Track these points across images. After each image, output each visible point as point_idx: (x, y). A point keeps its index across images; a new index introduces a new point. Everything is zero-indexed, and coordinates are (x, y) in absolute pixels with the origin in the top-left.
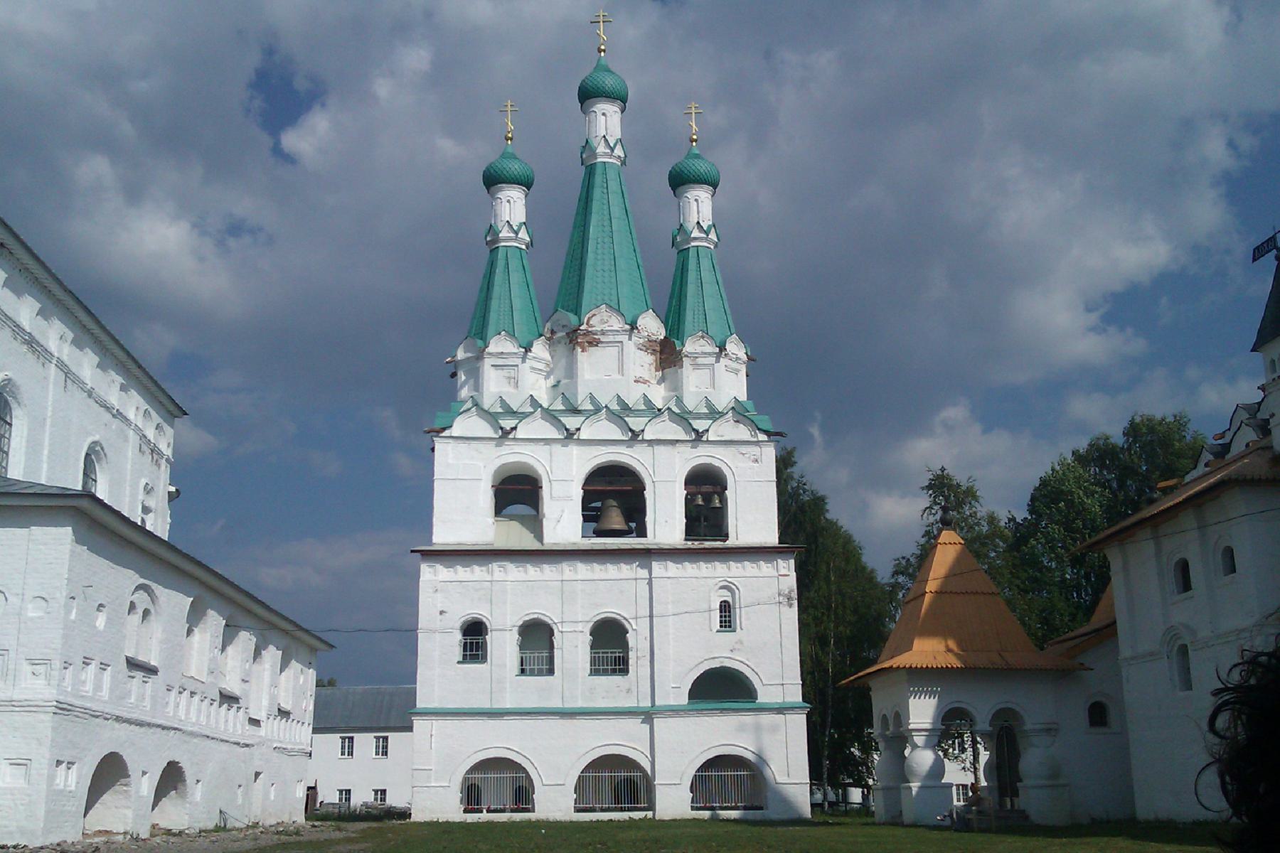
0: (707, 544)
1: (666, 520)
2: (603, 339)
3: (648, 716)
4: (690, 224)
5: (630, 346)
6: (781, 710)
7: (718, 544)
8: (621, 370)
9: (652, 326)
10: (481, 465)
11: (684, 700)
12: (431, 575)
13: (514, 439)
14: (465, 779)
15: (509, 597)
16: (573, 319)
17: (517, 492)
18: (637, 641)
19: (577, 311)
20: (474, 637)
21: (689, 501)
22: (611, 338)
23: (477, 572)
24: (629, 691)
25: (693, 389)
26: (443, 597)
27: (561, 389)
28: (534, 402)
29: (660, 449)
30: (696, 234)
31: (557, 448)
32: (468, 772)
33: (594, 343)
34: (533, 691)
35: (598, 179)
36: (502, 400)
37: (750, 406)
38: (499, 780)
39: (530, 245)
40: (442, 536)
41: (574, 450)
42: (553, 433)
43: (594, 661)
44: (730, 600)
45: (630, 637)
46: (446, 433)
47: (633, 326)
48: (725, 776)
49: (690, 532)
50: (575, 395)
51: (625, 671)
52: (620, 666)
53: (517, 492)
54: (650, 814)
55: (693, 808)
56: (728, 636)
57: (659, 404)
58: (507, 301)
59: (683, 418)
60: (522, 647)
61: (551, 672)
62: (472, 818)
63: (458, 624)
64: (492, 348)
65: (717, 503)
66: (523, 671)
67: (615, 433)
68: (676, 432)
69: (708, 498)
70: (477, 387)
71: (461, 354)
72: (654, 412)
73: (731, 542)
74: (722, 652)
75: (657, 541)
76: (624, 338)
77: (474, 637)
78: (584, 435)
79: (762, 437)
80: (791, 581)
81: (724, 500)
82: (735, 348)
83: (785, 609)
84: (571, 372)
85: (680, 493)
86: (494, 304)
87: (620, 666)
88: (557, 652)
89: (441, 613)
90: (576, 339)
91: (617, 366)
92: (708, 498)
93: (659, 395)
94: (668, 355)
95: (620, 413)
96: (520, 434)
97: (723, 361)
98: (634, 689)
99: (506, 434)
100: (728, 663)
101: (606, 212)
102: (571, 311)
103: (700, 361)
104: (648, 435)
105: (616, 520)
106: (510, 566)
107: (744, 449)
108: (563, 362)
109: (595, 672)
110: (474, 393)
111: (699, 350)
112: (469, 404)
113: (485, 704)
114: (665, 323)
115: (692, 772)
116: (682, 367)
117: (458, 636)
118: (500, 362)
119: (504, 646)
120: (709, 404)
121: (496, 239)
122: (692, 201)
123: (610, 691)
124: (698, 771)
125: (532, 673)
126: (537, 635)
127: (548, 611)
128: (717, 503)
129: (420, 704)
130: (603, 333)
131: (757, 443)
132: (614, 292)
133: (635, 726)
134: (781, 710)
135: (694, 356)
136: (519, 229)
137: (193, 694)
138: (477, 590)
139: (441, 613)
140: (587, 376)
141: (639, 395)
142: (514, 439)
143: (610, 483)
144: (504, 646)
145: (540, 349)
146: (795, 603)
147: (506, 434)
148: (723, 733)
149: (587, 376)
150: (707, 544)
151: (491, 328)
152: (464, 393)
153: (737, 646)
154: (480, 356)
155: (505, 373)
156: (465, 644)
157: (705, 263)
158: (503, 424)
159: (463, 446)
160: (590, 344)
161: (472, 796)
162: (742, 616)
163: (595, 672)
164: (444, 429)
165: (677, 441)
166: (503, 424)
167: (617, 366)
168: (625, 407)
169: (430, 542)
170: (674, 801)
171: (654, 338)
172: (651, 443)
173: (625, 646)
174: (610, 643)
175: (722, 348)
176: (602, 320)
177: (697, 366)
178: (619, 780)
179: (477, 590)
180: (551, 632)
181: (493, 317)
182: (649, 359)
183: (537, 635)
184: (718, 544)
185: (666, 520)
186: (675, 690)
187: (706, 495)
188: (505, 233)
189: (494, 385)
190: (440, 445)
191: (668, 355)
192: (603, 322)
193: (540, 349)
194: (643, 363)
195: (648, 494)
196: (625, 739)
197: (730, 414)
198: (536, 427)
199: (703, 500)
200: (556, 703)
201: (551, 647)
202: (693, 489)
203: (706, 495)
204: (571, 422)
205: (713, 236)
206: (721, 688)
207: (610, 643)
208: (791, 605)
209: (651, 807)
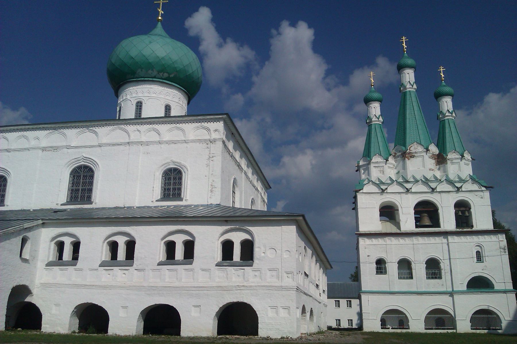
0: (465, 230)
1: (448, 220)
2: (416, 155)
3: (451, 294)
4: (445, 111)
5: (427, 157)
6: (505, 292)
7: (469, 230)
8: (424, 166)
9: (434, 149)
11: (465, 288)
12: (363, 242)
13: (387, 193)
14: (382, 317)
15: (394, 250)
16: (404, 148)
17: (388, 212)
18: (444, 266)
19: (404, 145)
21: (456, 214)
22: (419, 155)
23: (380, 241)
24: (442, 285)
25: (452, 172)
26: (369, 251)
27: (400, 174)
28: (391, 179)
29: (443, 195)
30: (447, 114)
31: (404, 196)
32: (383, 314)
33: (413, 157)
34: (405, 285)
35: (408, 97)
36: (379, 179)
38: (396, 317)
39: (383, 123)
40: (363, 228)
41: (410, 196)
42: (401, 190)
44: (480, 250)
45: (442, 265)
46: (361, 191)
47: (427, 150)
49: (458, 225)
50: (407, 176)
53: (388, 212)
54: (455, 331)
55: (472, 329)
57: (439, 178)
59: (450, 182)
61: (411, 278)
63: (375, 261)
64: (374, 160)
65: (467, 214)
67: (425, 189)
68: (449, 188)
70: (369, 174)
71: (361, 163)
72: (440, 181)
73: (474, 229)
75: (445, 229)
76: (424, 154)
77: (381, 266)
79: (484, 189)
80: (504, 243)
81: (470, 213)
82: (467, 156)
84: (404, 167)
85: (453, 211)
86: (372, 145)
88: (414, 271)
90: (405, 155)
93: (438, 174)
94: (441, 160)
95: (426, 182)
96: (389, 190)
97: (463, 161)
99: (383, 191)
100: (481, 274)
101: (412, 109)
102: (402, 145)
103: (454, 161)
104: (438, 189)
105: (427, 221)
106: (393, 239)
107: (477, 193)
108: (401, 163)
109: (428, 278)
110: (368, 177)
111: (453, 157)
112: (366, 182)
113: (388, 290)
115: (470, 315)
116: (447, 164)
117: (375, 265)
118: (377, 165)
119: (392, 268)
120: (459, 177)
121: (371, 121)
122: (445, 102)
123: (434, 285)
125: (404, 278)
126: (405, 265)
127: (410, 256)
128: (467, 214)
129: (363, 289)
130: (416, 153)
131: (482, 191)
133: (447, 299)
134: (505, 292)
135: (451, 160)
139: (368, 256)
142: (387, 193)
144: (392, 268)
145: (391, 160)
146: (507, 251)
147: (383, 191)
150: (465, 230)
151: (372, 154)
152: (363, 177)
154: (369, 163)
155: (379, 169)
157: (452, 125)
158: (381, 187)
159: (368, 196)
160: (411, 157)
161: (383, 323)
163: (428, 278)
164: (360, 190)
165: (450, 191)
166: (381, 187)
168: (426, 179)
169: (359, 231)
170: (464, 326)
172: (440, 192)
173: (439, 268)
174: (433, 267)
175: (463, 156)
176: (415, 148)
177: (452, 163)
181: (372, 150)
182: (433, 161)
183: (405, 265)
184: (469, 230)
185: (448, 220)
187: (463, 211)
188: (374, 119)
189: (375, 173)
190: (359, 196)
191: (441, 160)
192: (415, 149)
193: (391, 160)
194: (431, 163)
195: (440, 211)
196: (443, 303)
197: (470, 180)
199: (462, 213)
200: (414, 289)
202: (457, 209)
203: (463, 211)
204: (408, 186)
205: (454, 115)
206: (480, 284)
207: (433, 267)
208: (505, 252)
209: (455, 328)
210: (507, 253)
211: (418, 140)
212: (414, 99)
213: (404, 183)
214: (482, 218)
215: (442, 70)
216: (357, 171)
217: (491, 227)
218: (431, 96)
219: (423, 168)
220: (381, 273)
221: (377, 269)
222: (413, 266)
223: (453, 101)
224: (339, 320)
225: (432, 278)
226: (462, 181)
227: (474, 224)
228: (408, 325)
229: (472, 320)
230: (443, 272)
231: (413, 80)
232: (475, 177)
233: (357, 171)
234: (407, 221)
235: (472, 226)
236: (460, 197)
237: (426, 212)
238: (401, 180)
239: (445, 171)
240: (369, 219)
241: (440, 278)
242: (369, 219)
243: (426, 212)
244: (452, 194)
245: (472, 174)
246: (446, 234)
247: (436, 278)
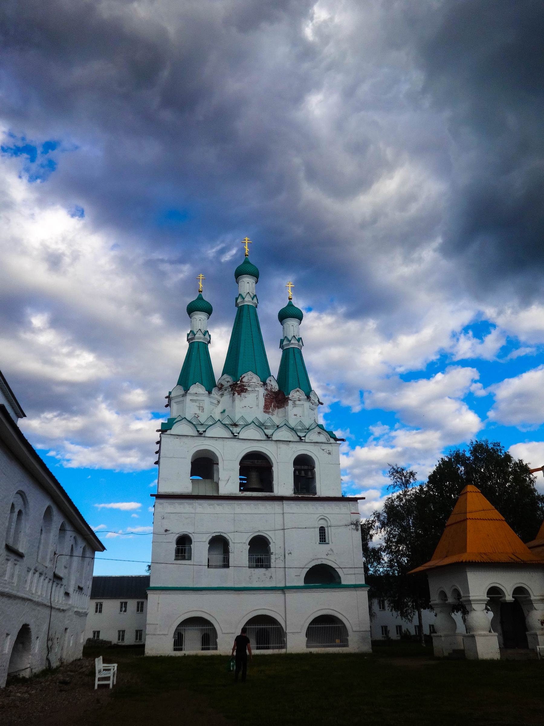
1: (283, 481)
11: (302, 583)
14: (176, 629)
27: (226, 413)
34: (216, 577)
43: (250, 560)
45: (272, 546)
46: (168, 432)
51: (268, 567)
56: (324, 547)
61: (226, 565)
62: (179, 654)
74: (320, 555)
78: (241, 436)
81: (313, 474)
88: (231, 556)
96: (208, 434)
98: (274, 577)
100: (325, 562)
104: (275, 438)
115: (307, 625)
116: (287, 405)
118: (195, 398)
119: (200, 549)
122: (291, 326)
124: (310, 624)
134: (355, 587)
137: (41, 574)
138: (186, 519)
139: (166, 531)
144: (200, 549)
148: (323, 602)
150: (306, 496)
153: (330, 553)
155: (197, 404)
159: (177, 441)
165: (290, 441)
171: (273, 390)
185: (283, 481)
198: (218, 431)
202: (298, 467)
204: (235, 430)
206: (322, 576)
216: (167, 406)
220: (184, 558)
222: (231, 547)
225: (257, 567)
228: (216, 644)
233: (167, 406)
234: (229, 479)
237: (256, 471)
238: (227, 422)
239: (286, 415)
241: (268, 567)
243: (256, 471)
244: (291, 445)
246: (281, 499)
247: (262, 567)
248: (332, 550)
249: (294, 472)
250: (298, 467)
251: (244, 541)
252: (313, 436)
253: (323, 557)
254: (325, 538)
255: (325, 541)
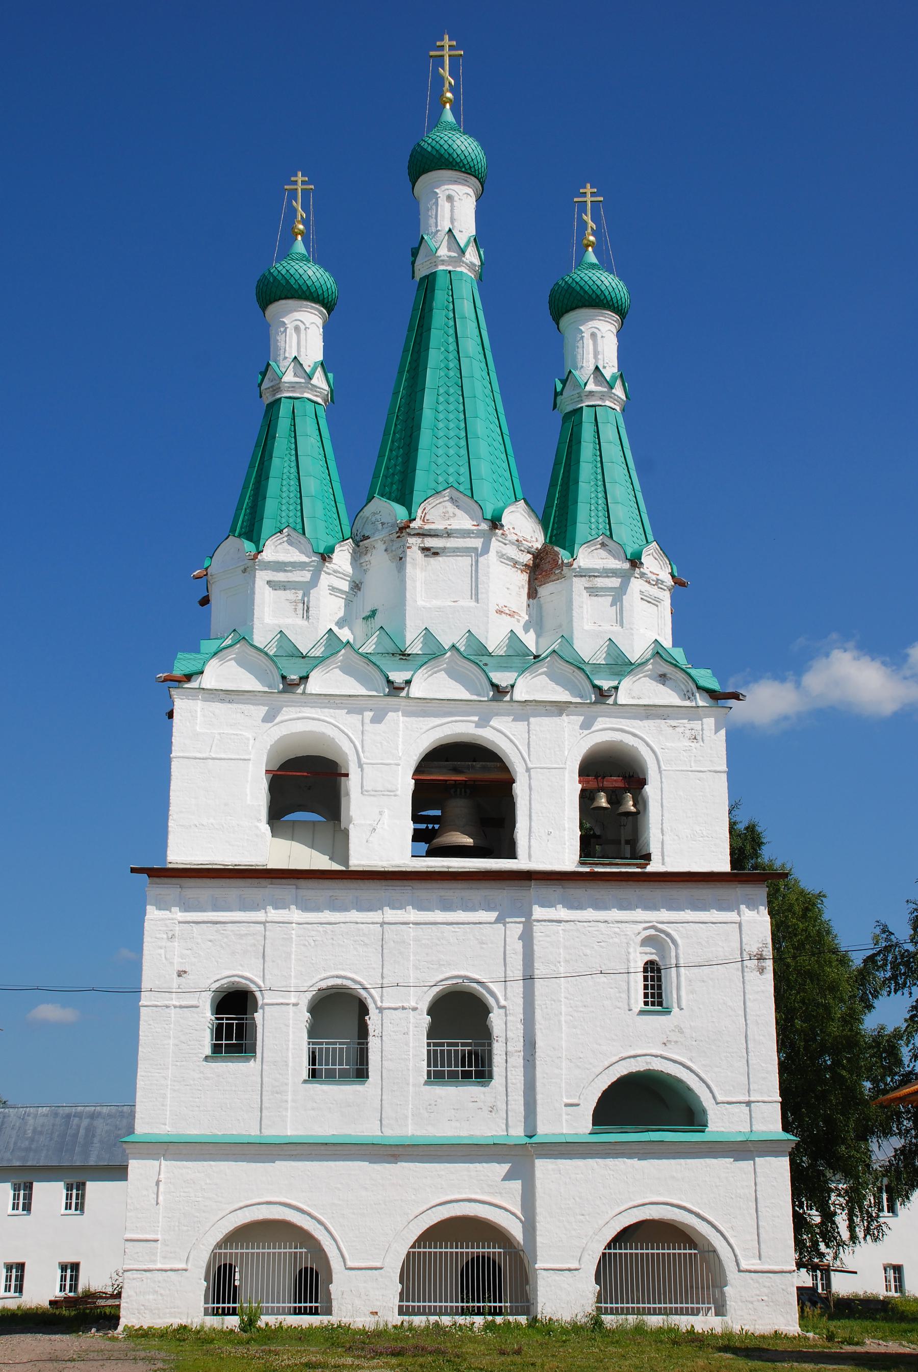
1: (548, 831)
4: (584, 373)
8: (475, 595)
9: (523, 527)
10: (249, 735)
14: (214, 1256)
16: (400, 512)
18: (505, 1026)
19: (404, 497)
20: (234, 1017)
32: (219, 1245)
35: (440, 297)
37: (679, 655)
40: (181, 852)
43: (433, 1058)
45: (496, 1020)
48: (656, 1256)
52: (476, 1067)
58: (294, 482)
60: (313, 1032)
61: (361, 1074)
66: (314, 1074)
69: (615, 799)
74: (646, 1046)
77: (234, 1017)
79: (701, 701)
81: (641, 802)
82: (655, 564)
83: (752, 976)
85: (573, 788)
86: (272, 486)
87: (476, 1067)
88: (373, 1043)
89: (180, 974)
91: (466, 583)
92: (615, 799)
96: (315, 685)
100: (658, 1065)
101: (452, 347)
109: (436, 1077)
114: (544, 523)
115: (598, 1248)
118: (281, 577)
119: (283, 1029)
122: (586, 335)
125: (331, 1077)
126: (340, 1016)
128: (630, 806)
129: (144, 1127)
132: (464, 470)
136: (314, 370)
138: (241, 936)
140: (420, 603)
141: (503, 633)
143: (456, 770)
144: (283, 1029)
146: (769, 965)
147: (289, 686)
149: (420, 603)
151: (267, 525)
153: (673, 1038)
156: (219, 1028)
158: (288, 675)
162: (681, 984)
163: (436, 1077)
164: (188, 677)
167: (466, 583)
168: (483, 651)
173: (485, 1034)
174: (461, 1029)
177: (593, 591)
178: (474, 1264)
179: (241, 936)
180: (363, 1010)
183: (340, 1016)
185: (548, 831)
186: (568, 1111)
187: (613, 790)
190: (182, 705)
192: (445, 516)
194: (506, 584)
195: (520, 790)
196: (483, 1192)
199: (609, 802)
201: (363, 1032)
203: (613, 790)
206: (645, 1105)
207: (461, 1029)
208: (762, 970)
210: (769, 976)
211: (465, 479)
212: (466, 307)
213: (389, 665)
214: (687, 827)
215: (589, 199)
217: (724, 865)
218: (536, 303)
219: (473, 604)
221: (218, 1032)
222: (373, 1021)
223: (619, 334)
224: (75, 1267)
226: (621, 665)
227: (654, 849)
229: (605, 1269)
230: (498, 1049)
231: (467, 228)
232: (679, 655)
235: (648, 857)
236: (607, 731)
237: (465, 795)
240: (216, 808)
242: (216, 808)
243: (465, 795)
245: (667, 643)
248: (681, 1032)
249: (586, 797)
250: (593, 785)
251: (413, 1004)
252: (635, 690)
253: (654, 1052)
254: (660, 996)
255: (660, 1004)
